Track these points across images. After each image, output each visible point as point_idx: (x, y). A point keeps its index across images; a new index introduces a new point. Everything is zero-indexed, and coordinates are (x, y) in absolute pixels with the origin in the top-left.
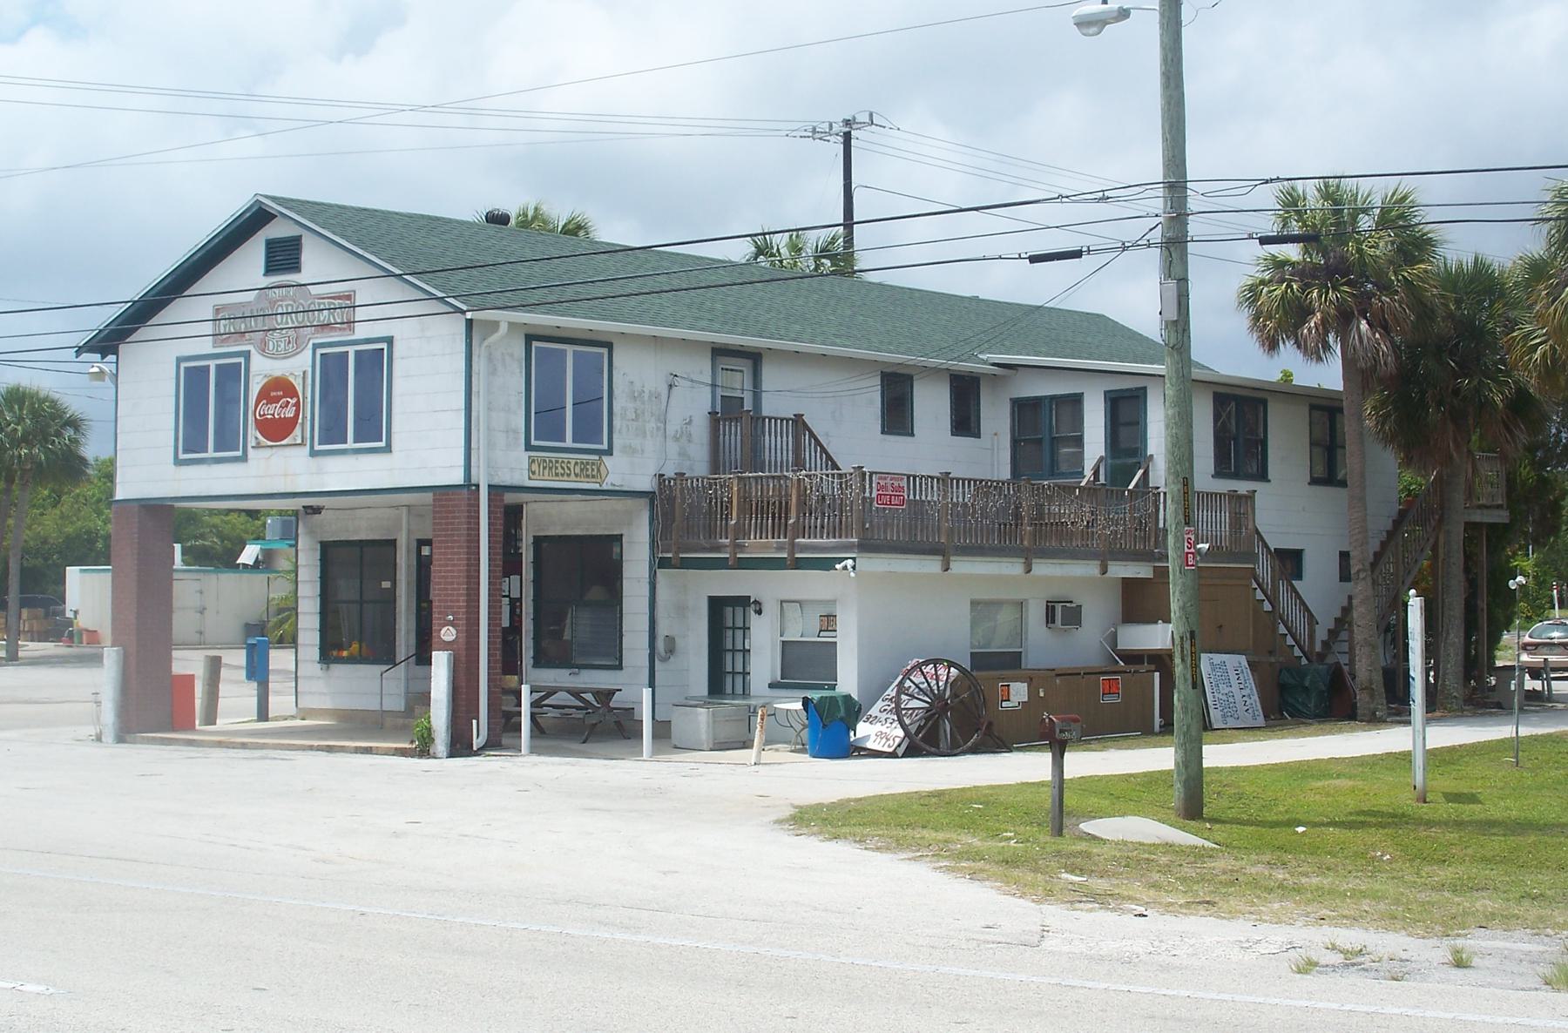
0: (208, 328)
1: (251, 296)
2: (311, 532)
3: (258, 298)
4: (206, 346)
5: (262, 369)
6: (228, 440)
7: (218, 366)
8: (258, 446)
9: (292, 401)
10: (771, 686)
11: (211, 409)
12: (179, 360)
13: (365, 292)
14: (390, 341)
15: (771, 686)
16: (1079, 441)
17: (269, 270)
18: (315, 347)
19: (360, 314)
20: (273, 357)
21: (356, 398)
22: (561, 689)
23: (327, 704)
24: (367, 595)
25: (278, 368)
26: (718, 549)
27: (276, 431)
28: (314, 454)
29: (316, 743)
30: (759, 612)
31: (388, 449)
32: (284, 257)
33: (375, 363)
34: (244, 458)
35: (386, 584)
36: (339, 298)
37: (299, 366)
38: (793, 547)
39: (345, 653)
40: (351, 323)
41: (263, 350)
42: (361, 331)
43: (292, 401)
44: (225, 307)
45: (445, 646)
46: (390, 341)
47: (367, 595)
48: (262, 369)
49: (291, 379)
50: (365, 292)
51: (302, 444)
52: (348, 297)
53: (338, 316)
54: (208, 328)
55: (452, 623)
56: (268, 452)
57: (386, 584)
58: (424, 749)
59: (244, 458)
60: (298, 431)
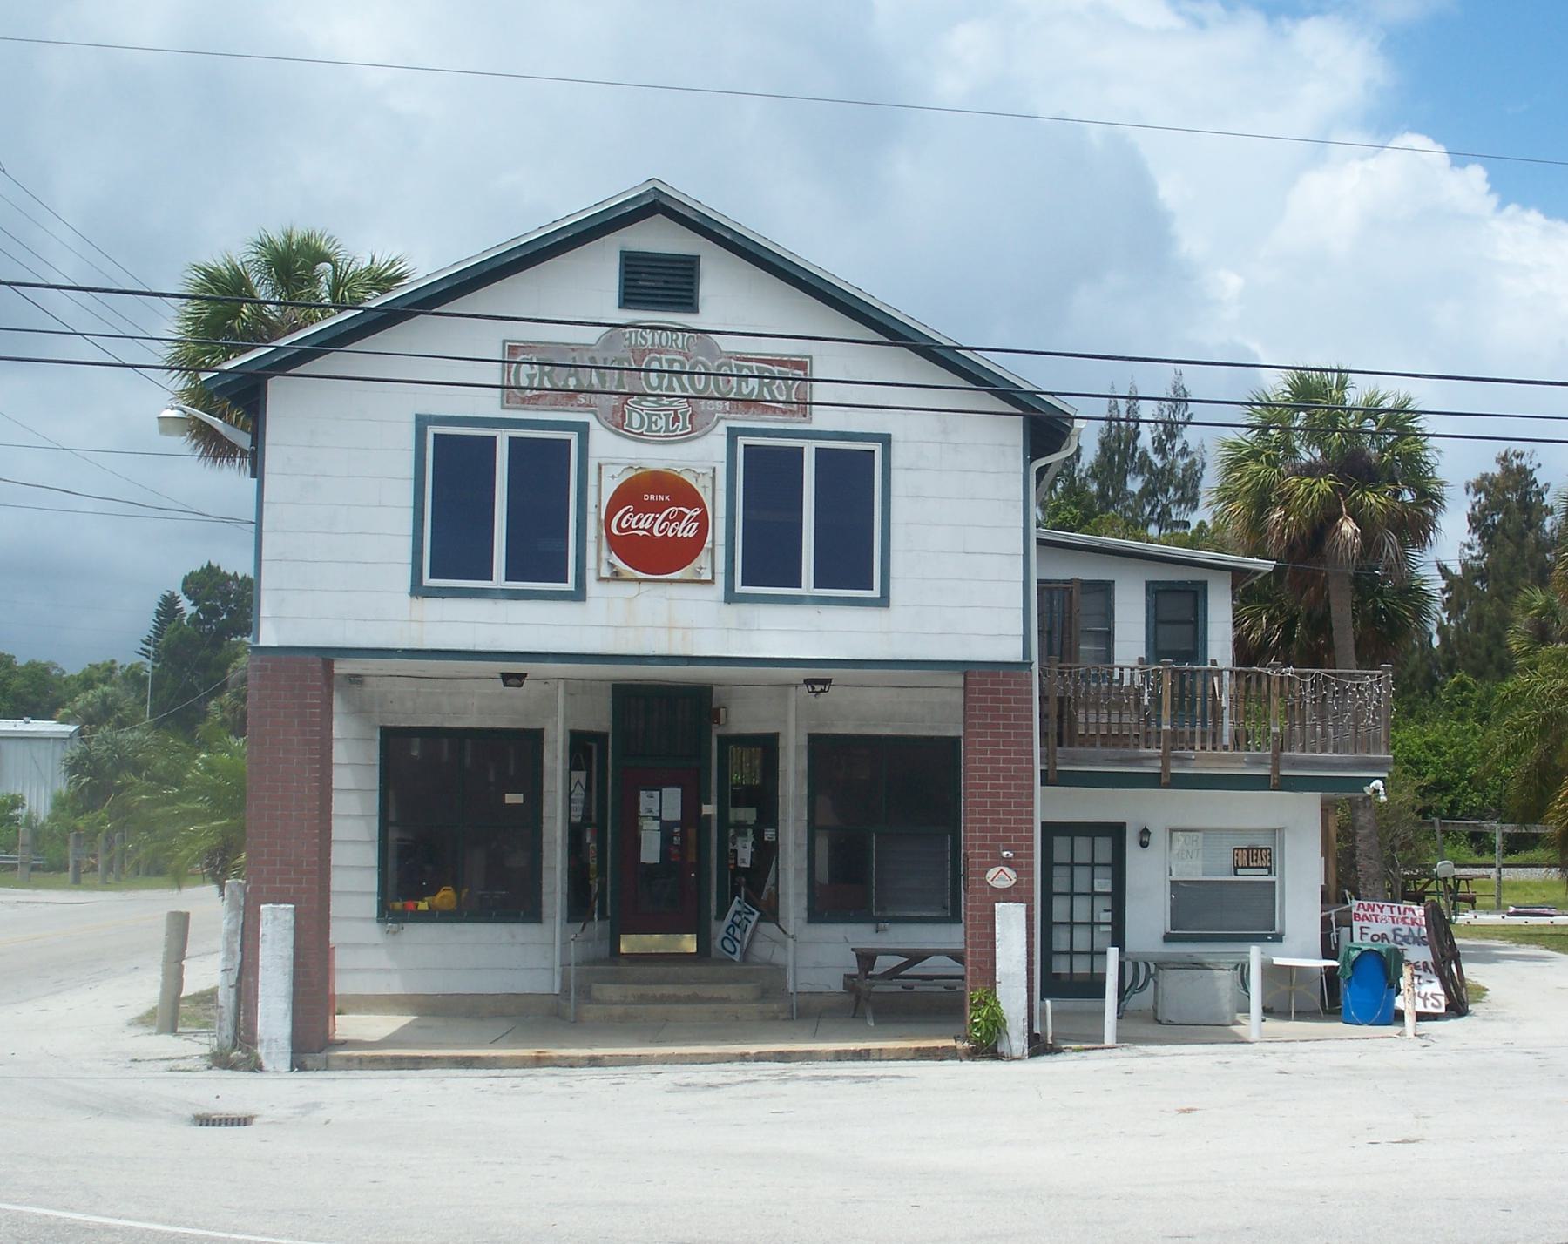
0: (493, 374)
1: (591, 336)
2: (360, 711)
3: (607, 342)
4: (488, 404)
5: (612, 457)
6: (541, 559)
7: (513, 441)
8: (616, 576)
9: (695, 513)
10: (1168, 938)
11: (492, 506)
12: (422, 422)
13: (827, 361)
14: (885, 440)
15: (1168, 938)
16: (1108, 637)
17: (629, 299)
18: (733, 434)
19: (820, 392)
20: (639, 438)
21: (812, 519)
22: (938, 952)
23: (396, 986)
24: (457, 819)
25: (656, 458)
26: (1138, 760)
27: (656, 558)
28: (731, 597)
29: (753, 1049)
30: (1144, 845)
31: (884, 601)
32: (659, 284)
33: (853, 477)
34: (579, 595)
35: (513, 798)
36: (781, 363)
37: (704, 459)
38: (1277, 762)
39: (423, 906)
40: (804, 405)
41: (618, 424)
42: (823, 420)
43: (695, 513)
44: (530, 346)
45: (1007, 895)
46: (885, 440)
47: (457, 819)
48: (612, 457)
49: (689, 478)
50: (827, 361)
51: (711, 582)
52: (801, 365)
53: (779, 391)
54: (493, 374)
55: (1008, 863)
56: (631, 589)
57: (513, 798)
58: (988, 1048)
59: (579, 595)
60: (703, 559)
